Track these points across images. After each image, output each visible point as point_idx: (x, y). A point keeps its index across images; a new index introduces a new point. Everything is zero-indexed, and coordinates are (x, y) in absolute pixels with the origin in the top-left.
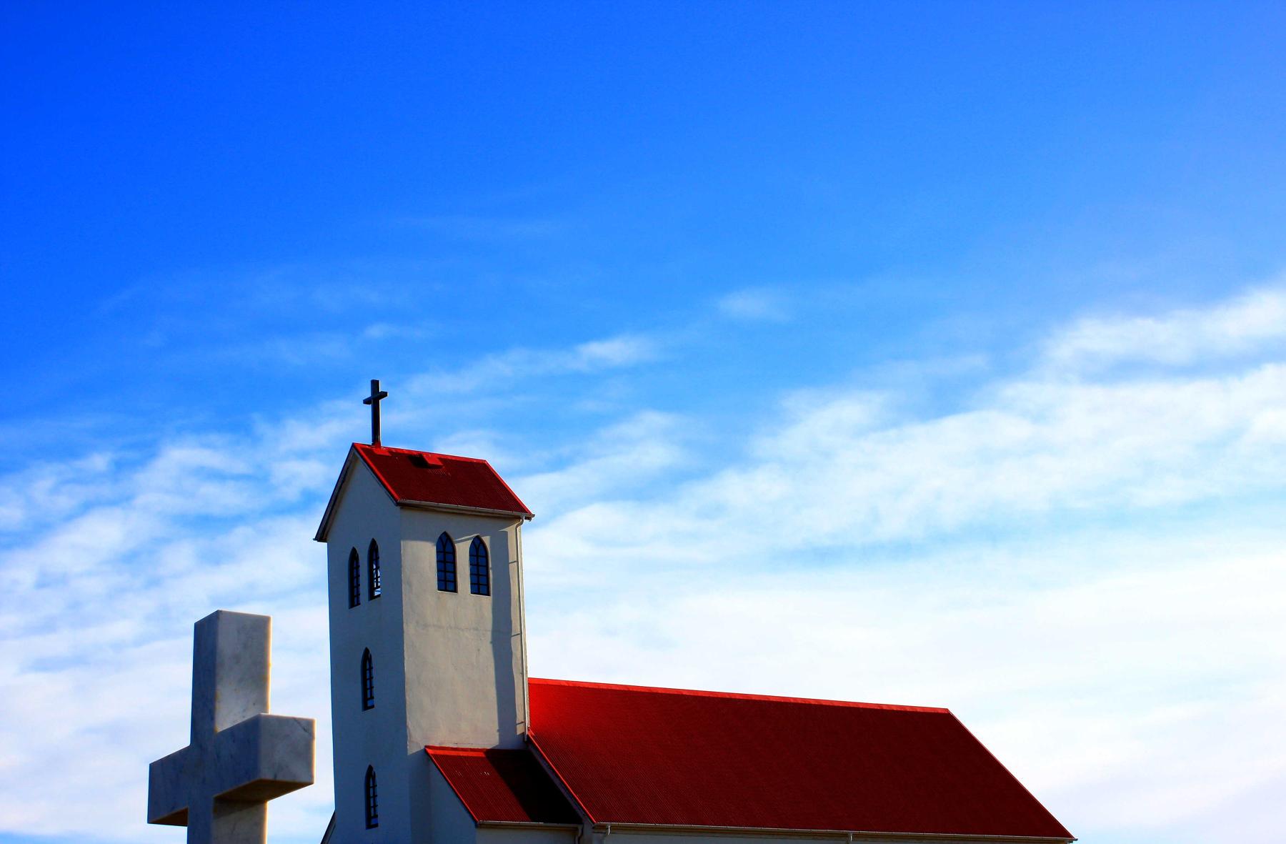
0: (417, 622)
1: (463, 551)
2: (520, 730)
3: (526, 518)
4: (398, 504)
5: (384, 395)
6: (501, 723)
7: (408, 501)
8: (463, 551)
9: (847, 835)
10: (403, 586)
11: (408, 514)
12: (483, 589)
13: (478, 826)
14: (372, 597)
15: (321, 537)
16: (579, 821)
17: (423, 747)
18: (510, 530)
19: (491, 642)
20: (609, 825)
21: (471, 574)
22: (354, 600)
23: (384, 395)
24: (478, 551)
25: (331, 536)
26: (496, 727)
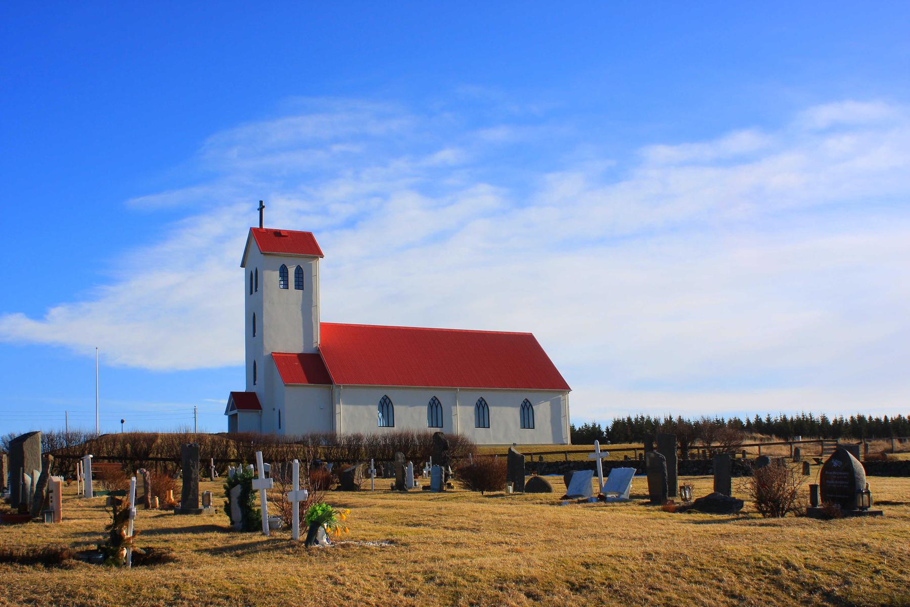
0: (270, 302)
1: (292, 272)
2: (315, 346)
3: (320, 257)
4: (261, 253)
5: (264, 207)
6: (305, 342)
7: (266, 252)
8: (292, 272)
9: (456, 389)
10: (264, 287)
11: (268, 257)
12: (301, 287)
13: (286, 385)
14: (256, 291)
15: (242, 266)
16: (331, 383)
17: (270, 353)
18: (313, 262)
19: (301, 310)
20: (342, 385)
21: (295, 281)
22: (251, 293)
23: (264, 207)
24: (299, 272)
25: (247, 264)
26: (303, 345)
